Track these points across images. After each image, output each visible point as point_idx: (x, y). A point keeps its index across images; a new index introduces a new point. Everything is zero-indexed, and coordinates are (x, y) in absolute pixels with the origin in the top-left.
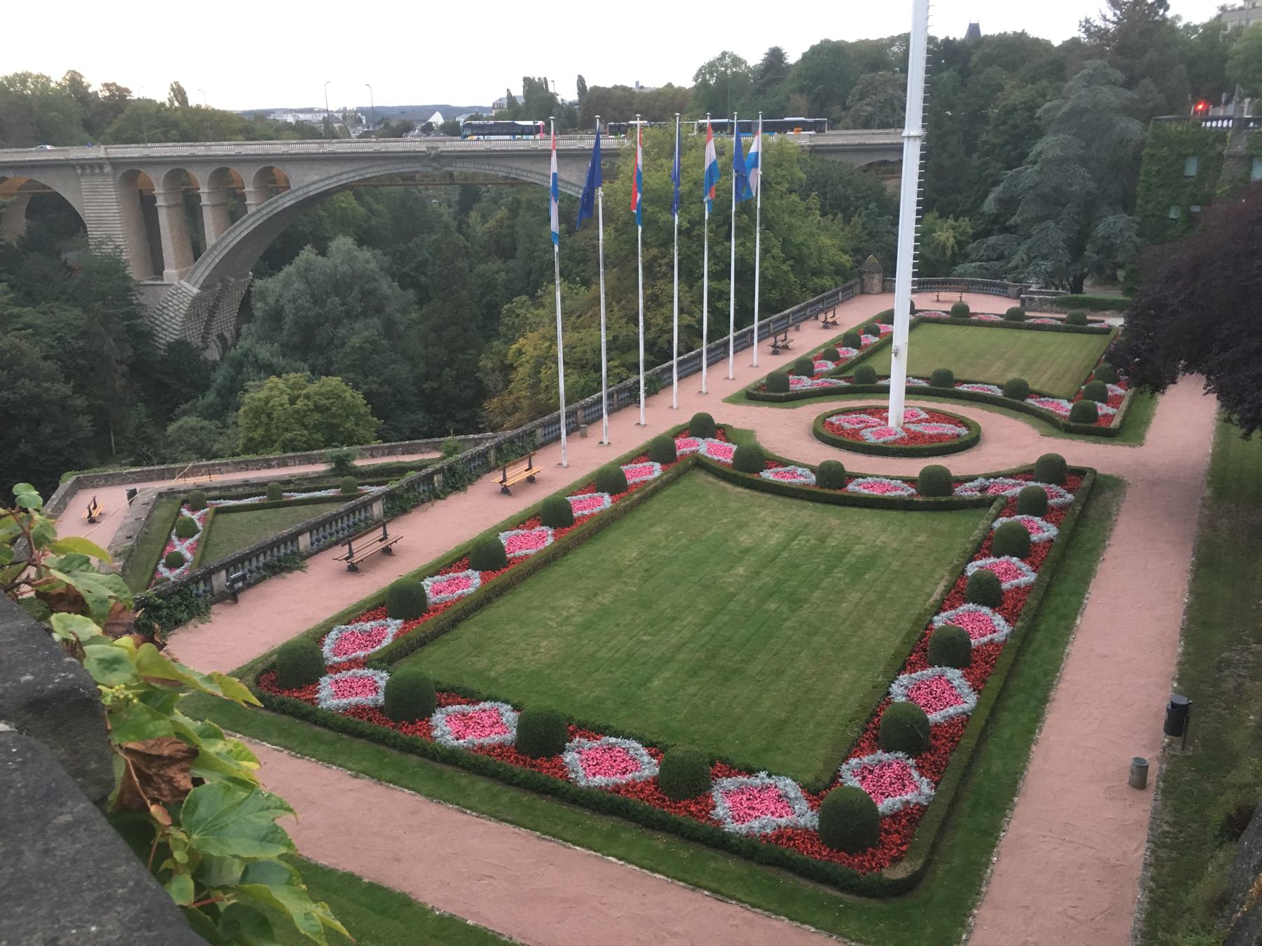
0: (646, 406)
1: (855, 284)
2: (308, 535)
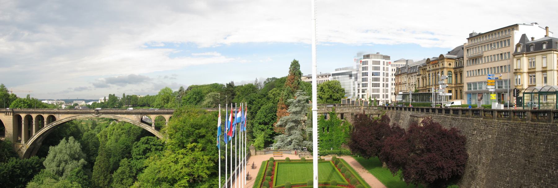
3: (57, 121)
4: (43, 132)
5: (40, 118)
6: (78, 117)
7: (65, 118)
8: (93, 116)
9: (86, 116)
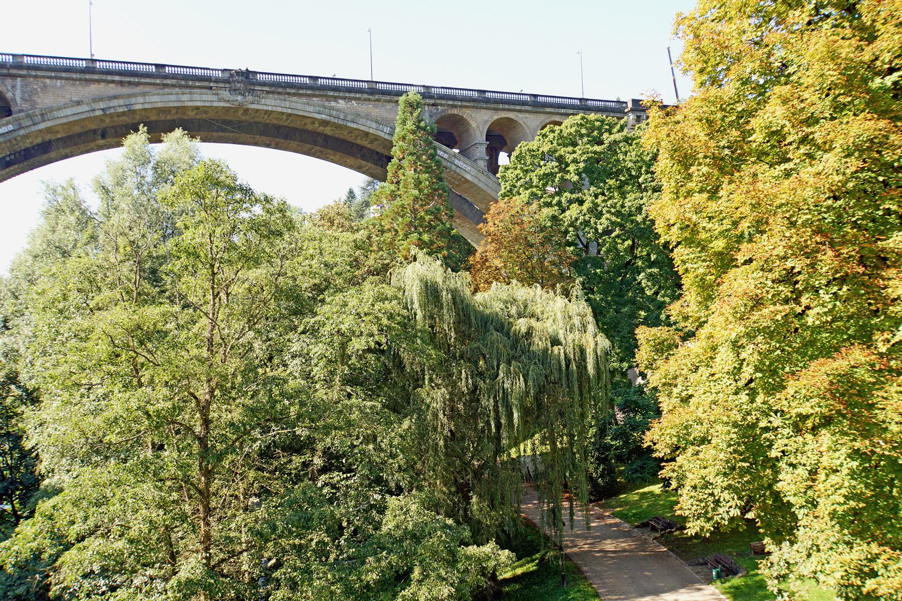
6: (140, 99)
8: (219, 100)
9: (185, 97)
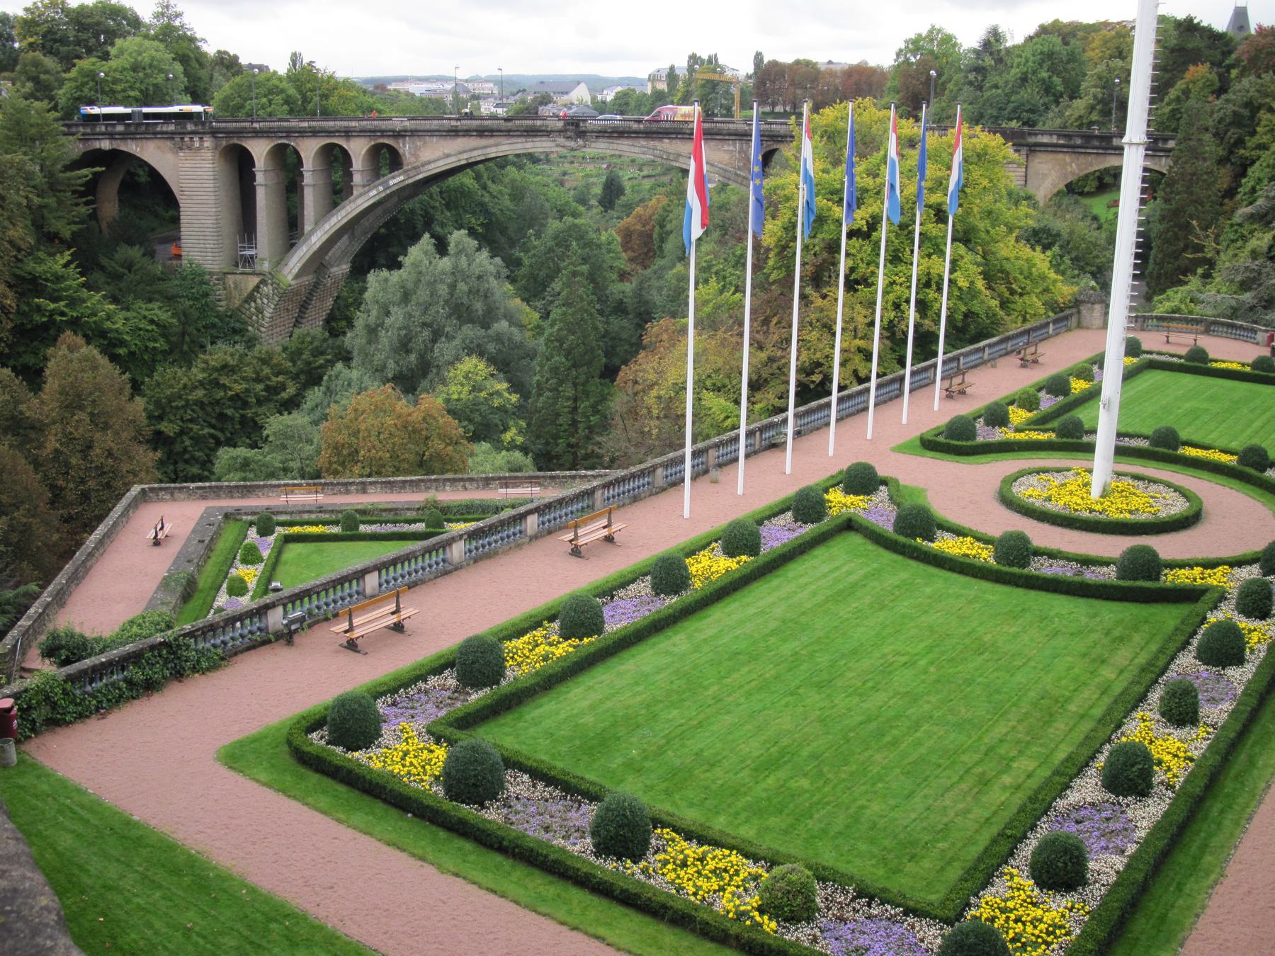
0: (793, 450)
1: (1071, 315)
2: (376, 573)
3: (405, 168)
4: (350, 216)
5: (335, 158)
6: (494, 149)
7: (439, 154)
8: (557, 146)
9: (529, 145)
